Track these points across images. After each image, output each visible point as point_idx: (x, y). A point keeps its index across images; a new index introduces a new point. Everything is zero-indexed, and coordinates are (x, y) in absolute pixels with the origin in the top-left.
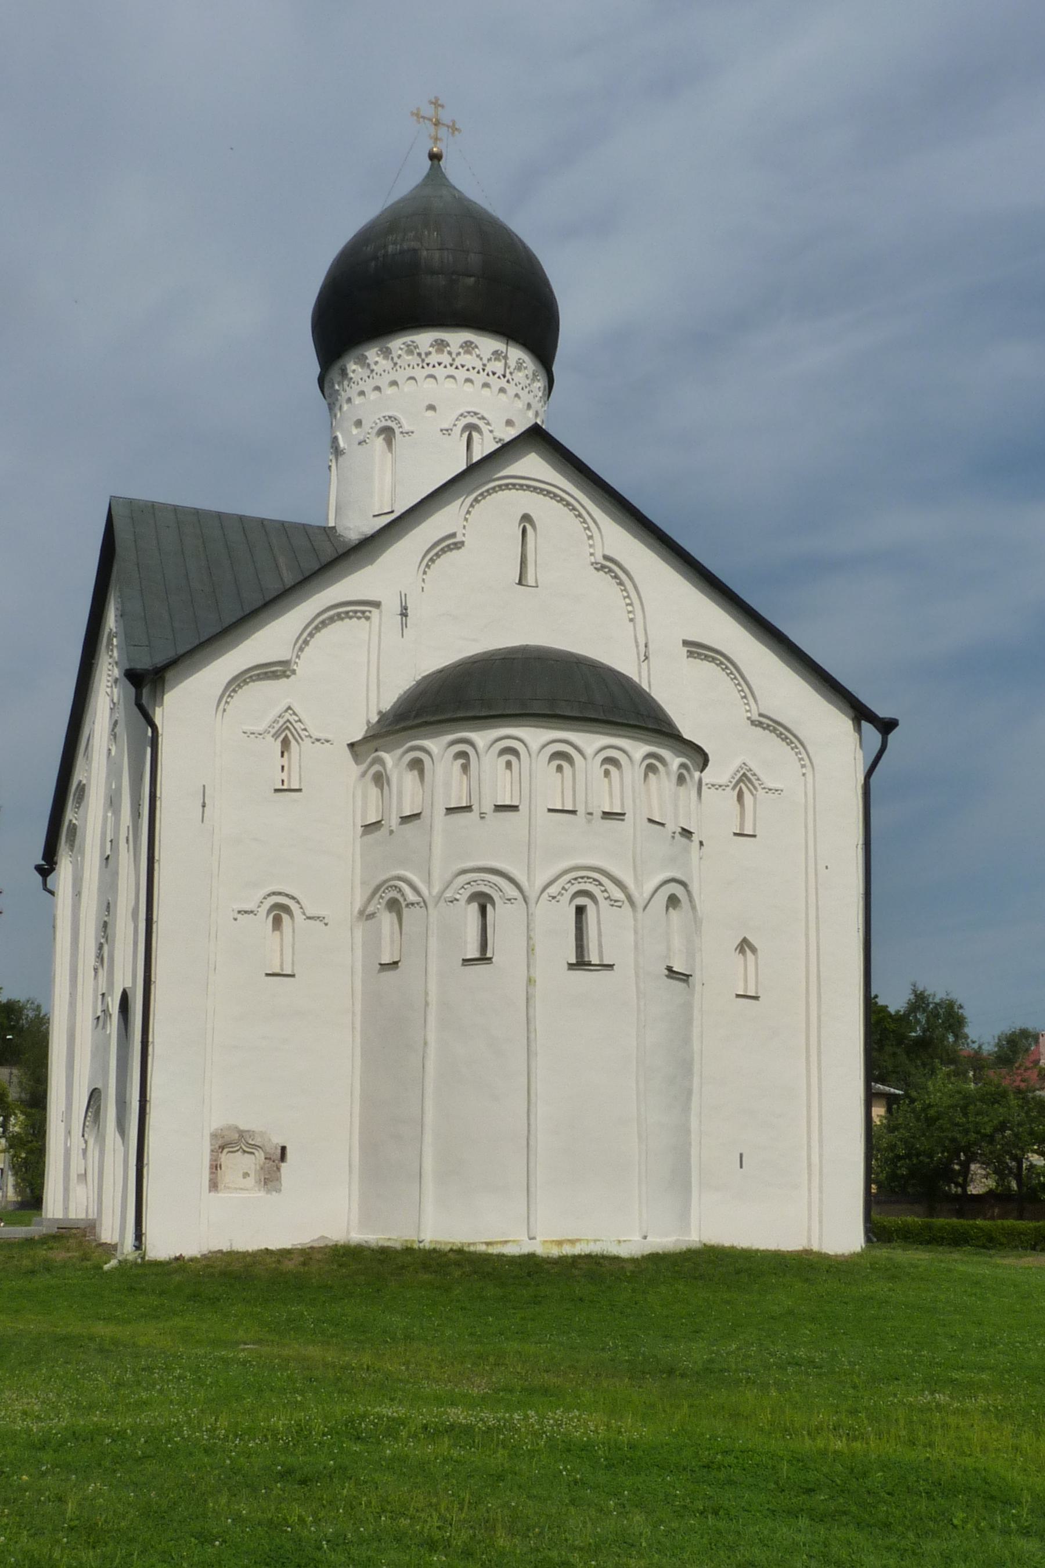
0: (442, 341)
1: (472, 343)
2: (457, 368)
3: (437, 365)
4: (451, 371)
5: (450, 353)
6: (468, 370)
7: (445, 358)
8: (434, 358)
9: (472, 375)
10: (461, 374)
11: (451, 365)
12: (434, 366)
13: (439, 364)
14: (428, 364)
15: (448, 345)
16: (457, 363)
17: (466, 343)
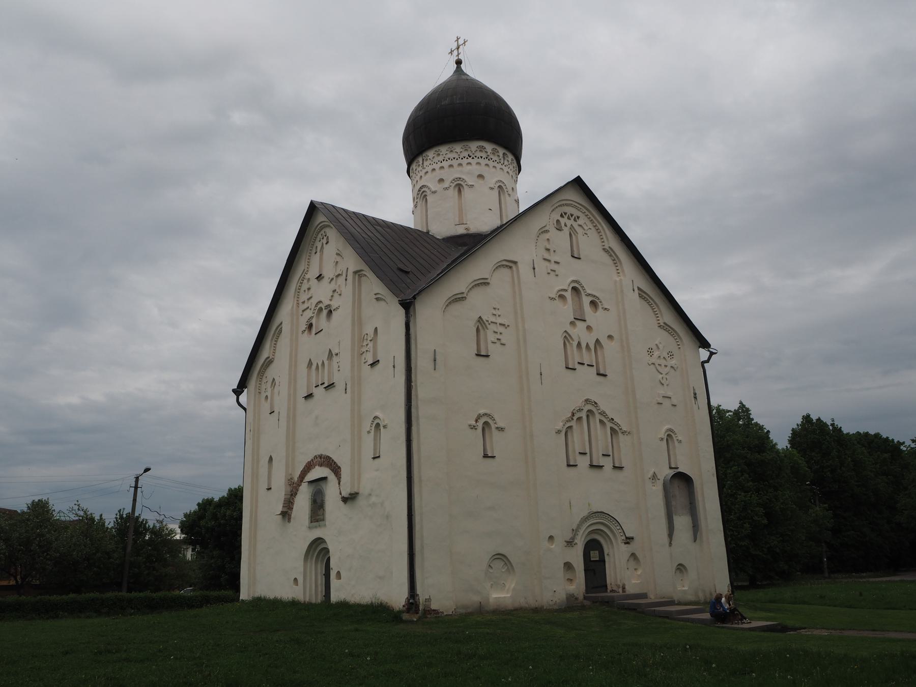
0: (483, 146)
1: (496, 149)
2: (489, 160)
3: (480, 158)
4: (486, 161)
5: (486, 152)
6: (493, 161)
7: (484, 155)
8: (479, 154)
9: (495, 164)
10: (491, 163)
11: (487, 158)
12: (478, 158)
13: (481, 157)
14: (476, 157)
15: (485, 148)
16: (489, 158)
17: (494, 149)
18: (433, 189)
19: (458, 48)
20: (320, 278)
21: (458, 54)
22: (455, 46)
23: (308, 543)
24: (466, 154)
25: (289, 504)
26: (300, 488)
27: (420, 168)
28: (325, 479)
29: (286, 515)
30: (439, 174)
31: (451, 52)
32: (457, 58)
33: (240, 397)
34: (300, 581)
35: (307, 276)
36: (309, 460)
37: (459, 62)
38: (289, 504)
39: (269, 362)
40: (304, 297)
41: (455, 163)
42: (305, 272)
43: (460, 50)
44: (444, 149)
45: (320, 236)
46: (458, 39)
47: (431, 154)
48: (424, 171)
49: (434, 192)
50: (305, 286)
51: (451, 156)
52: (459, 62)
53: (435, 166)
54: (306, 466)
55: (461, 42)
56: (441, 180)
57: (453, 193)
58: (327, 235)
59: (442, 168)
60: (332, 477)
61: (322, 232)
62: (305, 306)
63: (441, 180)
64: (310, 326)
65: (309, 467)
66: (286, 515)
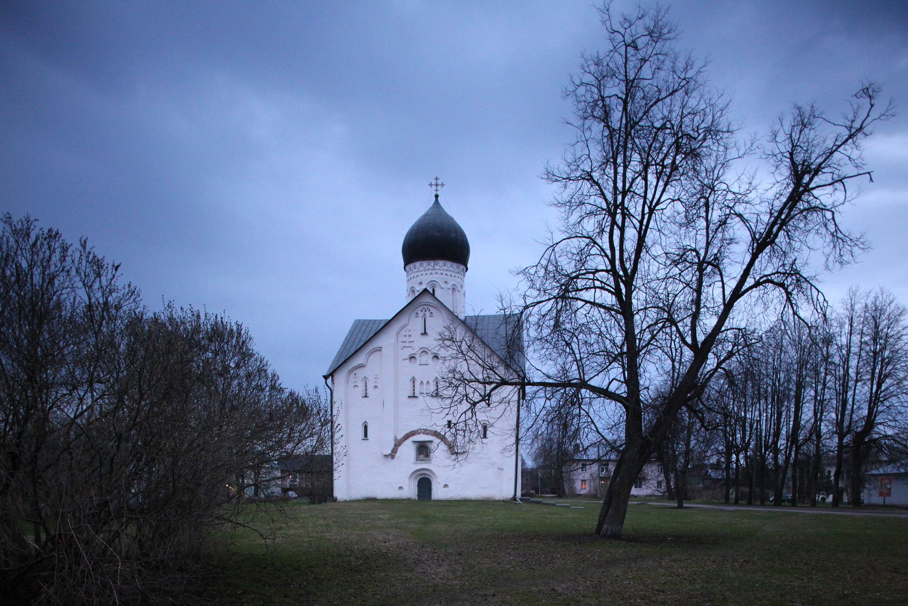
18: (443, 287)
19: (437, 185)
20: (425, 333)
21: (437, 190)
22: (434, 182)
23: (413, 471)
24: (457, 271)
25: (394, 451)
26: (404, 443)
27: (430, 267)
28: (431, 442)
29: (392, 455)
30: (448, 279)
31: (431, 185)
32: (435, 193)
33: (328, 380)
34: (406, 487)
35: (408, 327)
36: (414, 430)
37: (437, 196)
38: (394, 451)
39: (362, 366)
40: (402, 339)
41: (453, 274)
42: (405, 326)
43: (439, 187)
44: (449, 263)
45: (422, 308)
46: (437, 179)
47: (441, 263)
48: (434, 272)
49: (442, 288)
50: (403, 333)
51: (451, 269)
52: (437, 196)
53: (442, 271)
54: (411, 432)
55: (439, 182)
56: (446, 282)
57: (451, 291)
58: (431, 311)
59: (446, 274)
60: (436, 441)
61: (426, 307)
62: (407, 345)
63: (446, 282)
64: (412, 357)
65: (413, 433)
66: (392, 455)
